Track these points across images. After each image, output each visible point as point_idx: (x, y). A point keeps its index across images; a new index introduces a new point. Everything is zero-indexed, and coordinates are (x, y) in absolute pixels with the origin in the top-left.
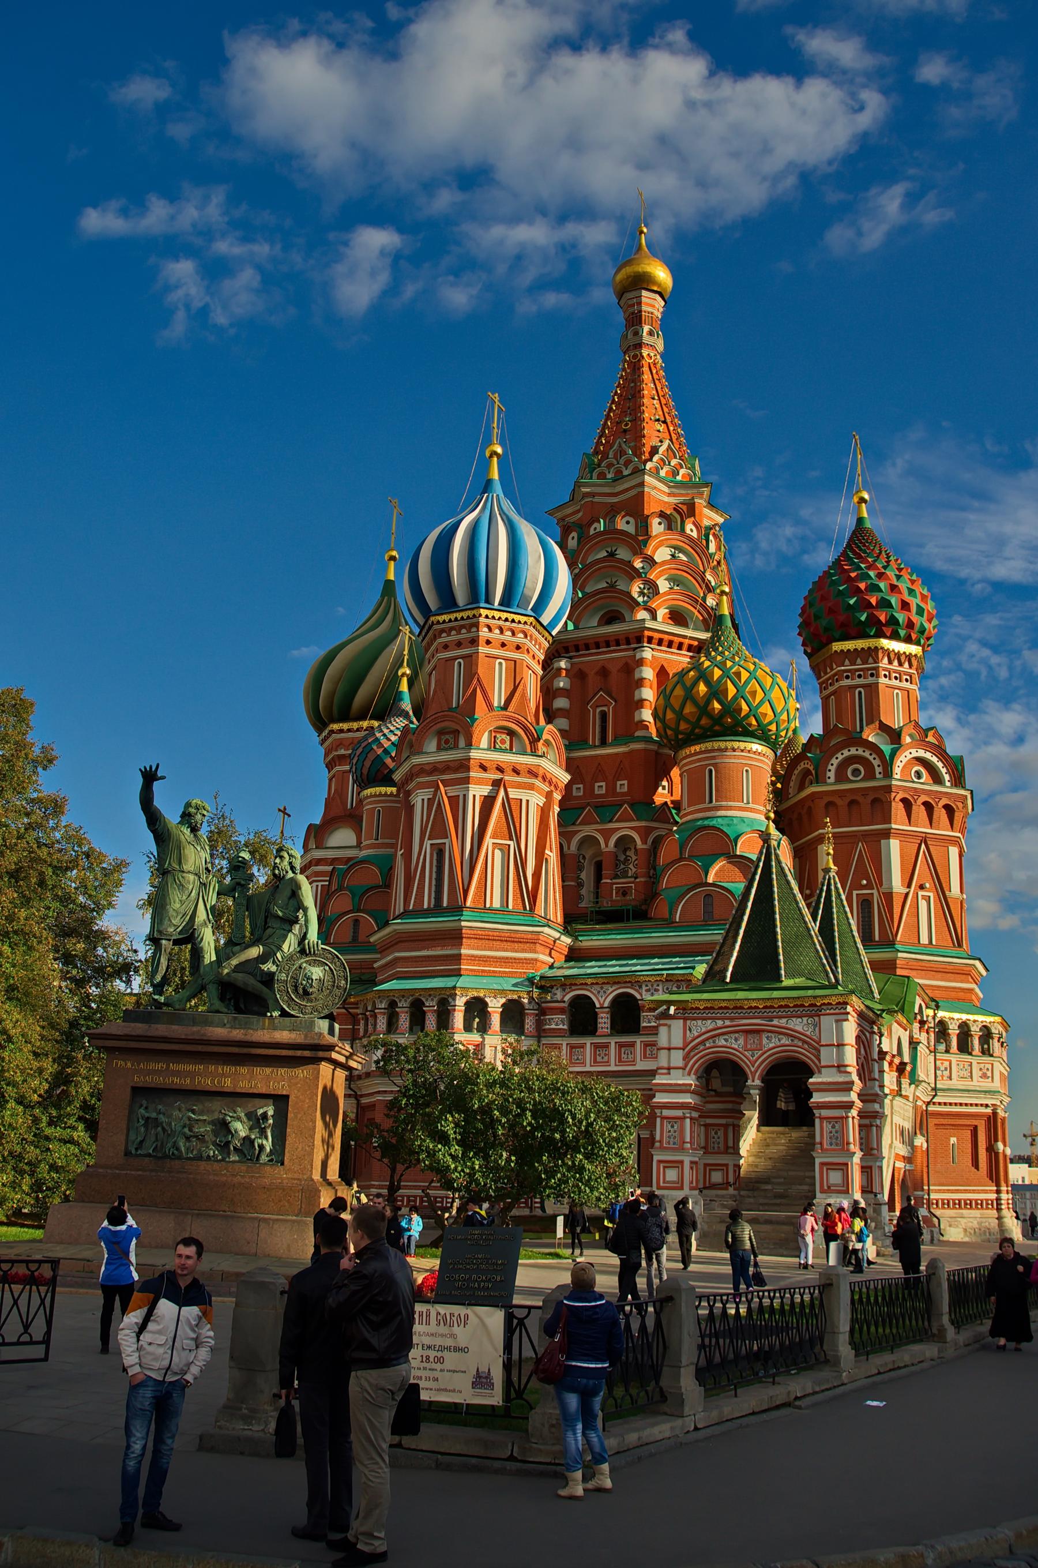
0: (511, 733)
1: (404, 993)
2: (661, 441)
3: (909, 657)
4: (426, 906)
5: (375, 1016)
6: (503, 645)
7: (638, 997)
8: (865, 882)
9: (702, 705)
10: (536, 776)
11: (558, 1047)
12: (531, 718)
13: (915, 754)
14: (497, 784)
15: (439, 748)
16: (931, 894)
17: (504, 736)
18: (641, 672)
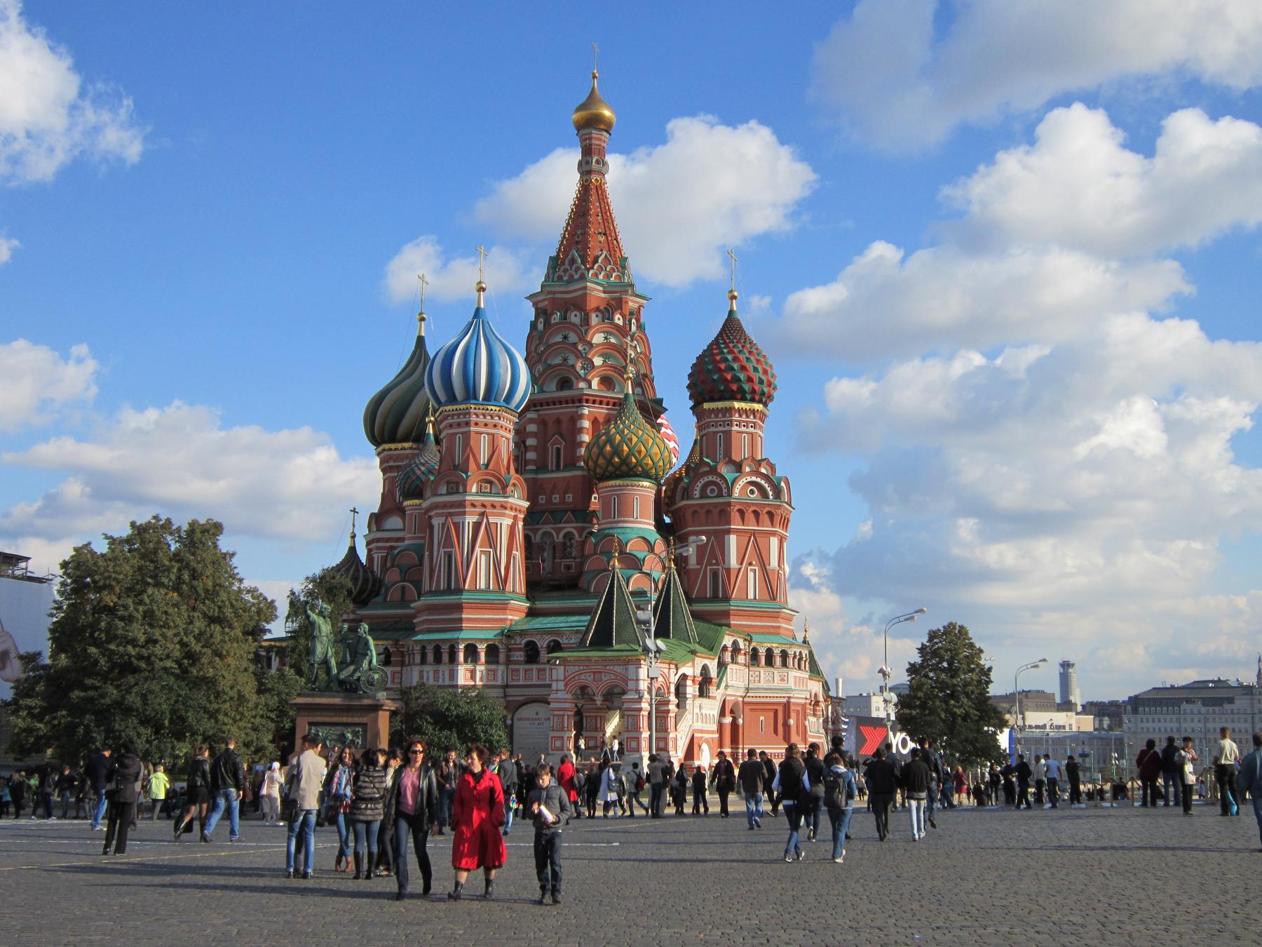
0: (491, 483)
1: (430, 641)
2: (602, 250)
3: (754, 412)
4: (442, 588)
5: (414, 654)
6: (486, 425)
7: (561, 641)
8: (714, 561)
9: (608, 457)
10: (506, 508)
11: (518, 670)
12: (503, 471)
13: (749, 479)
14: (482, 514)
16: (757, 568)
18: (581, 423)
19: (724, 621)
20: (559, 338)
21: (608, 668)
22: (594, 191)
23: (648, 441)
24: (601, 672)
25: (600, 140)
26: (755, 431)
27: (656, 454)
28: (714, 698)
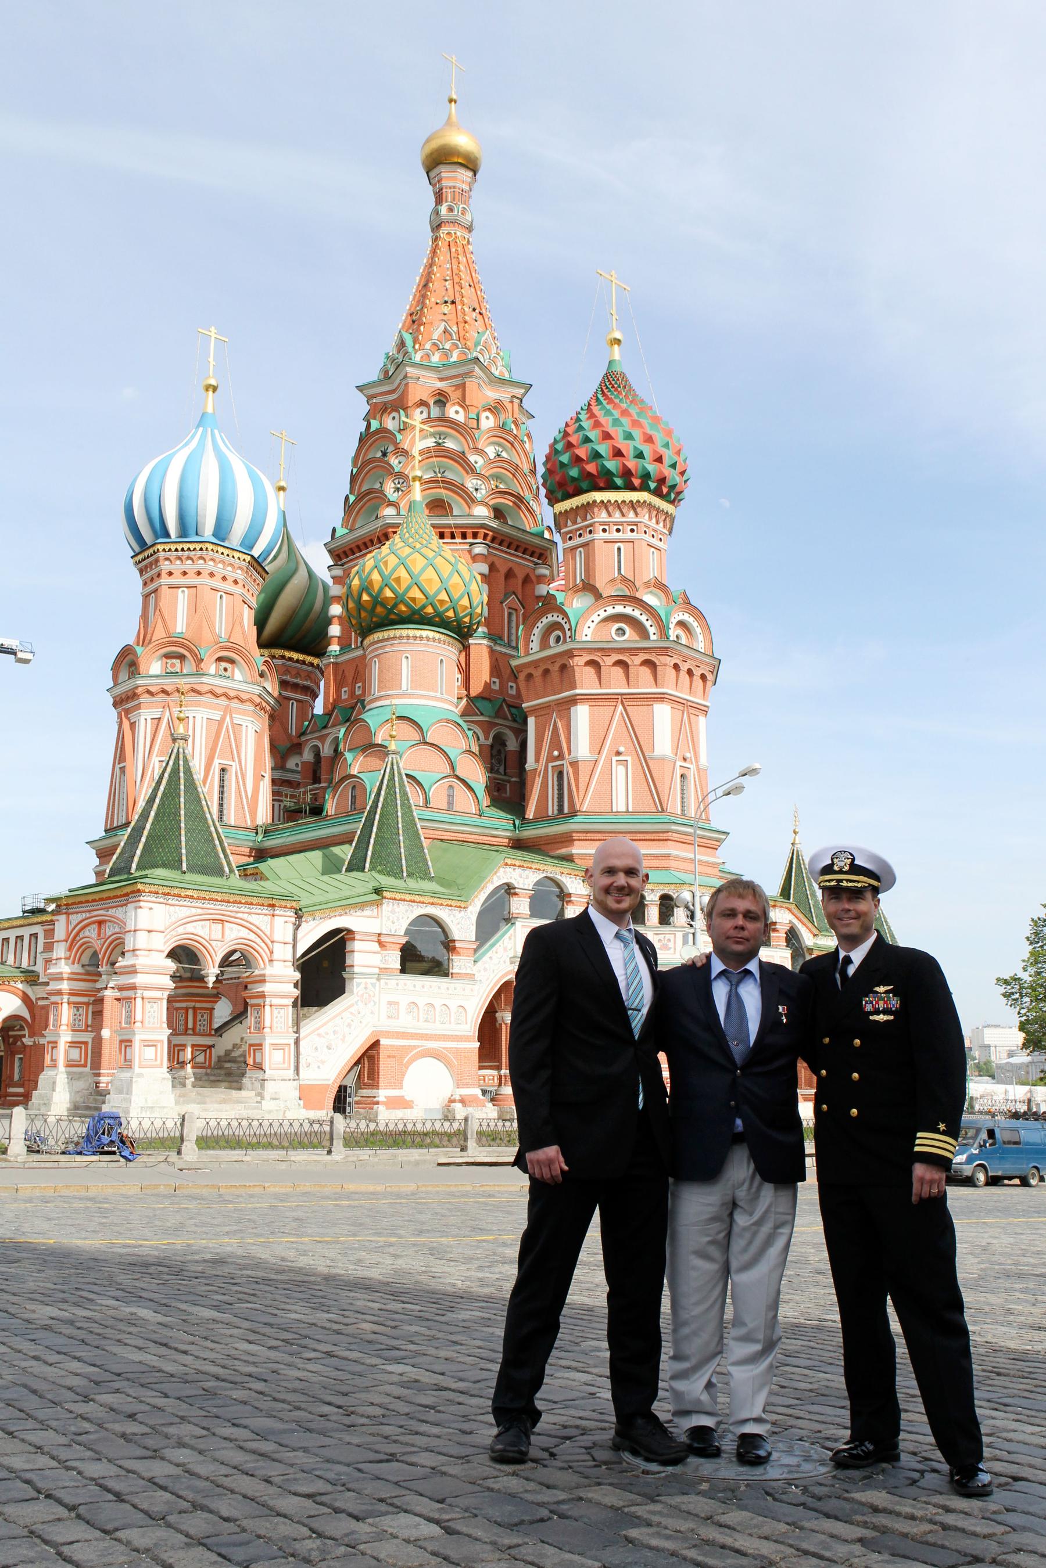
3: (633, 505)
6: (185, 573)
8: (556, 753)
10: (199, 693)
13: (610, 611)
15: (129, 678)
16: (629, 759)
17: (174, 661)
19: (563, 851)
20: (379, 454)
21: (111, 912)
22: (445, 249)
23: (414, 561)
24: (105, 921)
25: (454, 179)
26: (639, 536)
27: (430, 581)
28: (471, 977)
